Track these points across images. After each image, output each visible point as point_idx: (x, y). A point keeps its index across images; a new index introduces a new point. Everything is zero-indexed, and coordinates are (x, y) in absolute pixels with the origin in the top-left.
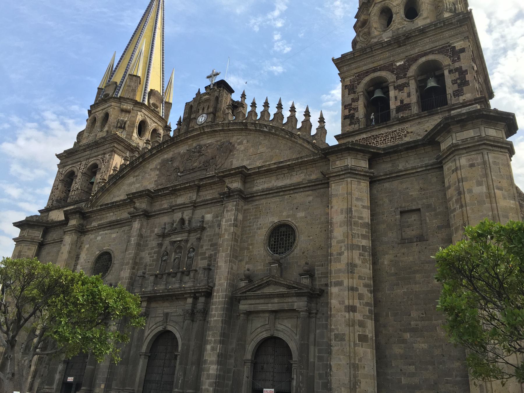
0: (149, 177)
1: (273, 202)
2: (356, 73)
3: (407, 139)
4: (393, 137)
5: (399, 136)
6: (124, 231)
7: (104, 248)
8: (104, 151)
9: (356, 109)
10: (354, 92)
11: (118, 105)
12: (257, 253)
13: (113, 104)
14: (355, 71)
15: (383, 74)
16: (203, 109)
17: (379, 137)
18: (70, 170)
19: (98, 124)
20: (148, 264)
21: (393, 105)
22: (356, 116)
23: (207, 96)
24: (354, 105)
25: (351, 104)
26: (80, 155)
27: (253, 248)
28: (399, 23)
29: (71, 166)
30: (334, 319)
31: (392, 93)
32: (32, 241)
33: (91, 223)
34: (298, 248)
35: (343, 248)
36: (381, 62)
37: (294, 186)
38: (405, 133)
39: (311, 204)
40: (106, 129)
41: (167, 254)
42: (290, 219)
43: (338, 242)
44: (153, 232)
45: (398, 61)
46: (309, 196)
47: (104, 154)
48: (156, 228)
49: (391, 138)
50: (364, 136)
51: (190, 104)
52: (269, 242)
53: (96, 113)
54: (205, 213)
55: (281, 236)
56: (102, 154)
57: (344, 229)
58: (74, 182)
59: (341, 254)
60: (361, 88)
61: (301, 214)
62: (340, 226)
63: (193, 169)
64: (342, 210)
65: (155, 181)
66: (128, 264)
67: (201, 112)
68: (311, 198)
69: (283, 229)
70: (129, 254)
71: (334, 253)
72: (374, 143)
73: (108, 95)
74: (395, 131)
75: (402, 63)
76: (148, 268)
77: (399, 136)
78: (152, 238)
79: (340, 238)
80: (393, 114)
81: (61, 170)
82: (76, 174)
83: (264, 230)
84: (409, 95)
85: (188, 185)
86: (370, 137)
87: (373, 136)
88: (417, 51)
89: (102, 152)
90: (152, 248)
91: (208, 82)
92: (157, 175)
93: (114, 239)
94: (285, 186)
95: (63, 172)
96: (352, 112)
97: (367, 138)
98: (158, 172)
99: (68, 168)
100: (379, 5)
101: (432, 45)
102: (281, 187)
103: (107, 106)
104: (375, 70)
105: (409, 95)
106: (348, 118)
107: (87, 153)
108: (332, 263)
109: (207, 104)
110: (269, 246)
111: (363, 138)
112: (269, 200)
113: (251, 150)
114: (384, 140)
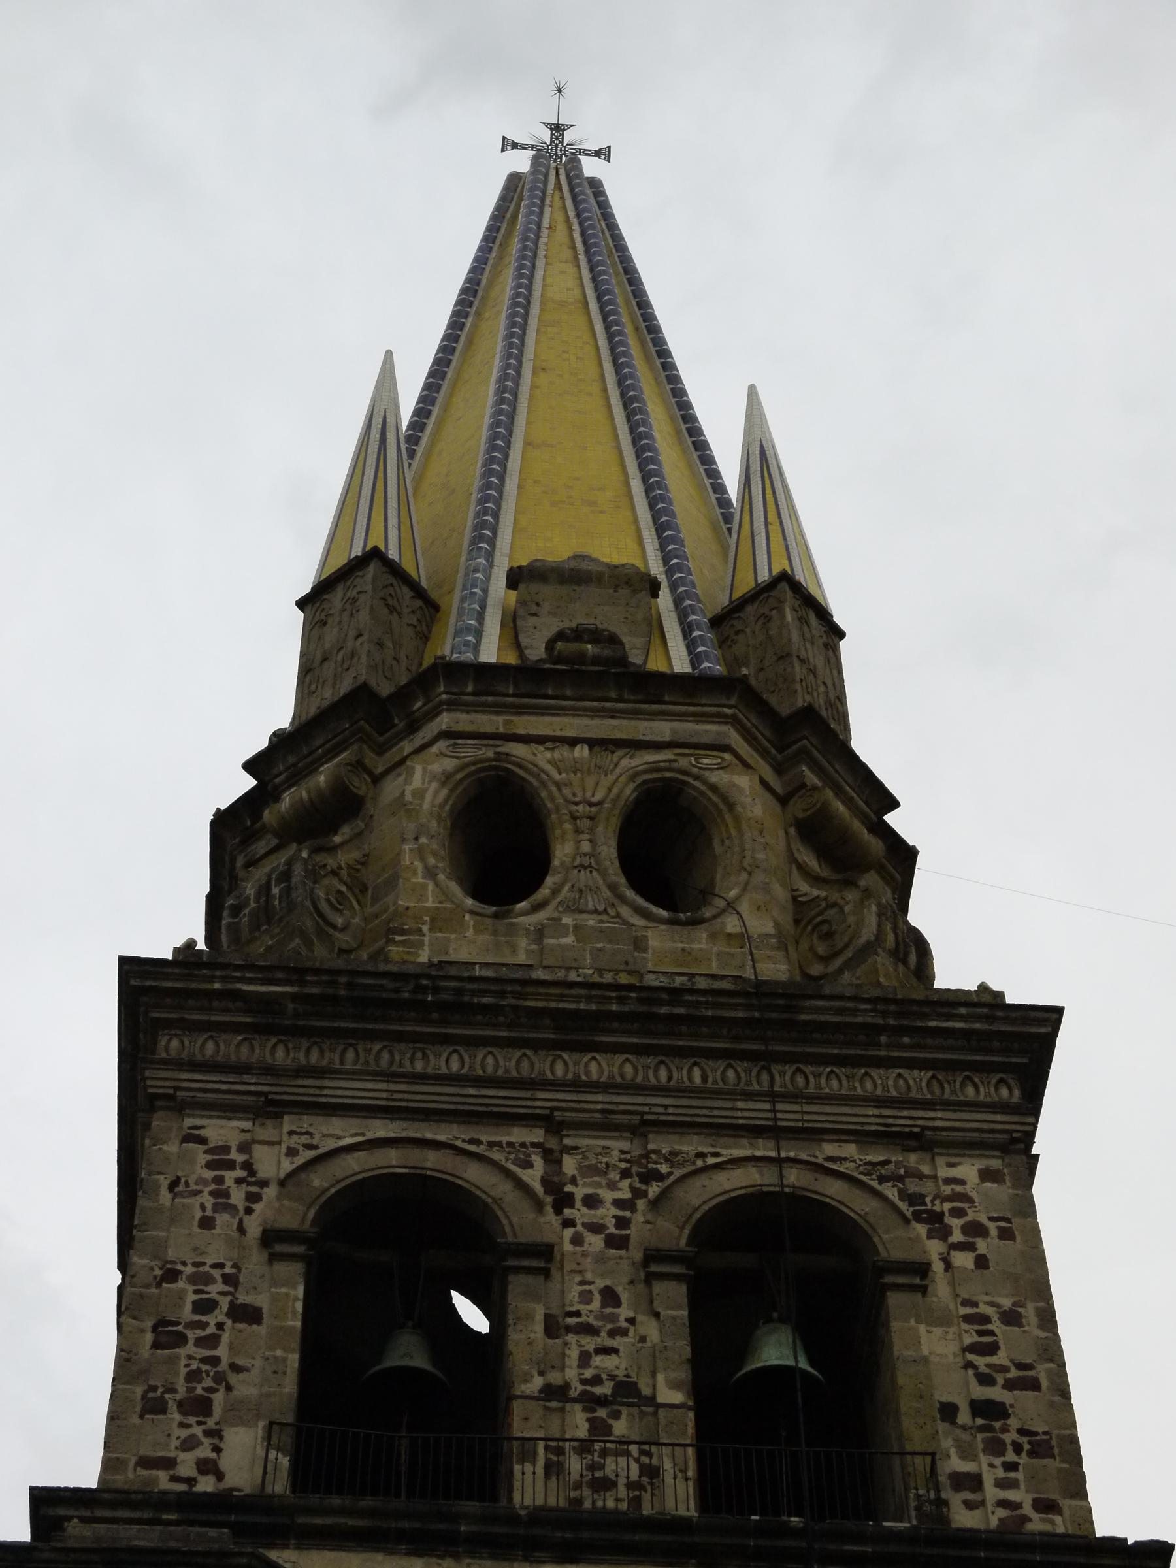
8: (903, 1119)
18: (392, 1160)
19: (583, 849)
53: (518, 750)
56: (863, 1137)
95: (271, 1163)
99: (347, 1146)
103: (663, 730)
107: (597, 1067)
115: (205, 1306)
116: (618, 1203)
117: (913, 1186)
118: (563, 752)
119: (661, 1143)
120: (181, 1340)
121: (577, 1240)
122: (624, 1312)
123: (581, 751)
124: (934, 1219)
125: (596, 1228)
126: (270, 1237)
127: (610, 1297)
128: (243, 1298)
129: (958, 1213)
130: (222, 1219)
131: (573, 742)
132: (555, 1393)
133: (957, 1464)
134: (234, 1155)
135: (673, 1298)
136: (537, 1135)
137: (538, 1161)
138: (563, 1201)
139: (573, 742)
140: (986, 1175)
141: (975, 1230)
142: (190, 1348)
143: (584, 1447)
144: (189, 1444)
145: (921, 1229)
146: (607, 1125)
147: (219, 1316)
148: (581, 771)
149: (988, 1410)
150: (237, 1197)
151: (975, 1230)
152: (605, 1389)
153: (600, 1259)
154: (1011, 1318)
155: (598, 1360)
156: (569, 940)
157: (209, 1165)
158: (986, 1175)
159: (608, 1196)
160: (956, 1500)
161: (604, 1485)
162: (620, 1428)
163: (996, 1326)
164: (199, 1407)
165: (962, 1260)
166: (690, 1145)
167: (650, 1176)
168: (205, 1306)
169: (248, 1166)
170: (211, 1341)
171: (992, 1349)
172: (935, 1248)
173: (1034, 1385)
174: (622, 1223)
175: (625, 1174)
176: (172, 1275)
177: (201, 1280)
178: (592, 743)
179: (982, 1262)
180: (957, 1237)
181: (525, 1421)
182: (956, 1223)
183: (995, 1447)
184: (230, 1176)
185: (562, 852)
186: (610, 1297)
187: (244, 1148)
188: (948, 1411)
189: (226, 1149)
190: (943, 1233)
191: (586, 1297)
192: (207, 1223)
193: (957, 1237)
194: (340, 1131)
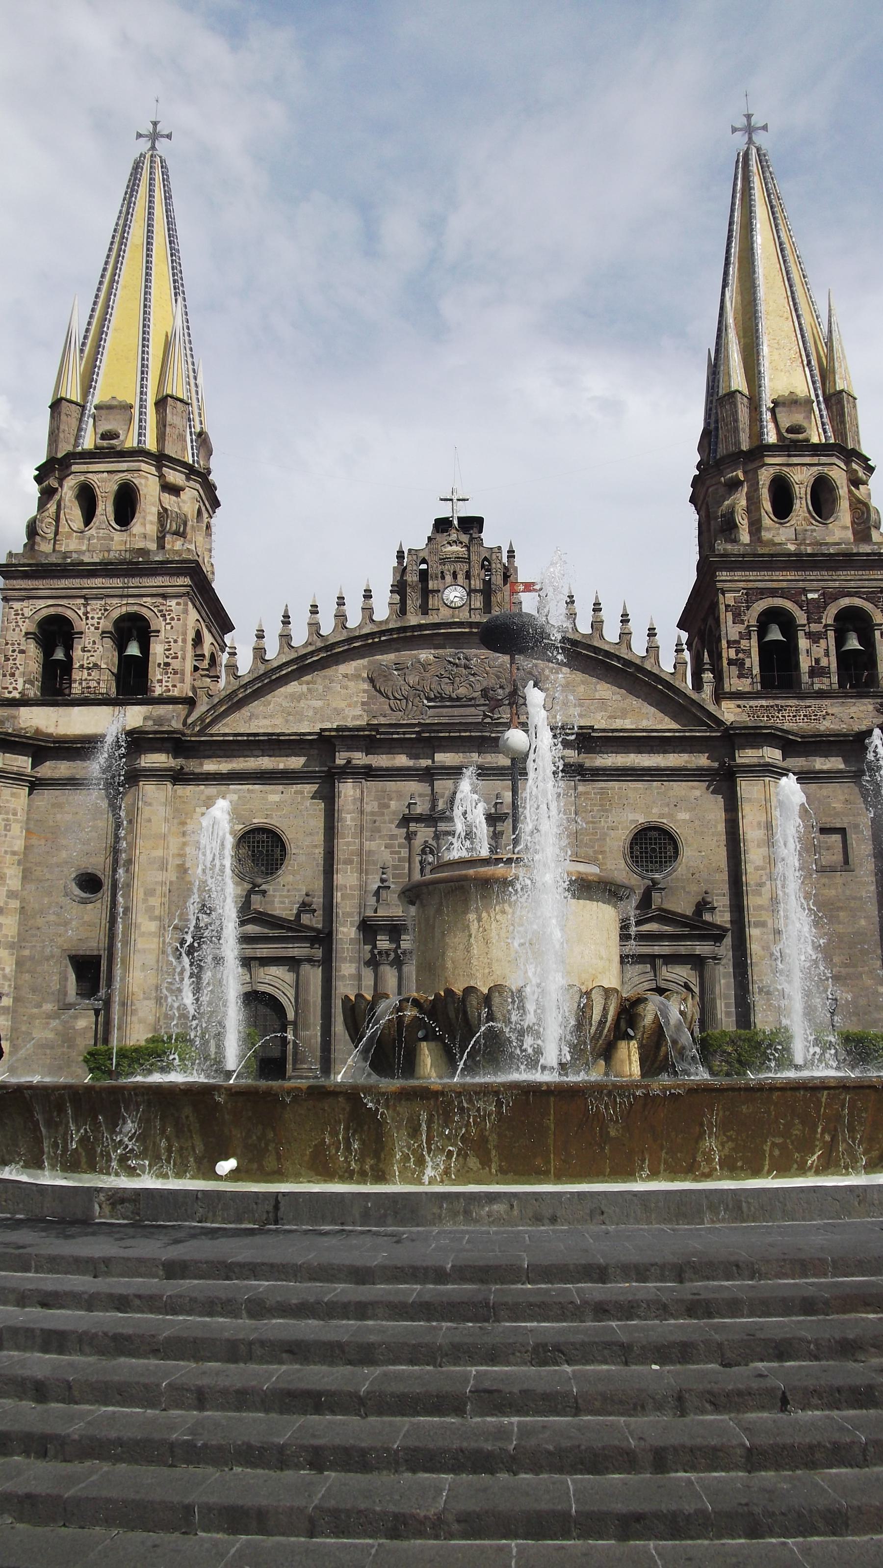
0: (343, 691)
1: (632, 789)
2: (744, 589)
3: (826, 725)
4: (804, 716)
5: (816, 715)
6: (302, 793)
7: (255, 821)
9: (748, 653)
10: (742, 622)
11: (153, 470)
12: (613, 867)
13: (144, 466)
14: (742, 585)
15: (788, 605)
16: (455, 575)
17: (785, 710)
18: (52, 611)
20: (390, 863)
21: (805, 664)
22: (748, 665)
23: (455, 548)
24: (744, 643)
25: (738, 642)
26: (77, 582)
27: (603, 858)
28: (805, 519)
29: (50, 602)
30: (755, 969)
31: (803, 643)
32: (17, 778)
33: (202, 765)
34: (683, 865)
35: (764, 878)
36: (784, 584)
37: (671, 770)
38: (824, 713)
39: (699, 802)
40: (136, 527)
41: (432, 852)
42: (665, 821)
43: (757, 869)
44: (388, 806)
45: (811, 591)
46: (693, 788)
47: (164, 596)
48: (391, 800)
49: (804, 716)
50: (764, 702)
51: (422, 555)
52: (632, 853)
53: (90, 476)
54: (503, 789)
55: (651, 844)
57: (764, 851)
58: (78, 647)
59: (761, 885)
60: (752, 616)
61: (683, 816)
62: (759, 846)
63: (458, 699)
64: (759, 823)
65: (363, 704)
66: (350, 862)
67: (449, 578)
68: (697, 793)
69: (655, 834)
70: (348, 844)
71: (752, 883)
72: (778, 717)
73: (115, 436)
74: (810, 707)
75: (816, 596)
76: (389, 871)
77: (816, 715)
78: (387, 818)
79: (759, 862)
80: (805, 678)
81: (17, 605)
82: (79, 625)
83: (620, 831)
84: (827, 654)
85: (468, 734)
86: (772, 706)
87: (777, 706)
88: (837, 584)
89: (154, 591)
90: (393, 837)
91: (445, 511)
92: (365, 691)
93: (278, 805)
94: (657, 769)
95: (28, 613)
96: (741, 655)
97: (767, 706)
98: (366, 686)
99: (41, 608)
100: (772, 470)
101: (860, 584)
102: (649, 769)
103: (124, 466)
104: (773, 593)
105: (827, 654)
106: (735, 665)
107: (98, 582)
108: (750, 897)
109: (466, 567)
110: (632, 857)
111: (762, 706)
112: (624, 785)
113: (582, 688)
114: (794, 716)
115: (14, 651)
116: (99, 618)
117: (161, 608)
118: (100, 475)
119: (109, 601)
120: (9, 659)
121: (89, 628)
122: (96, 646)
123: (105, 474)
124: (164, 616)
125: (92, 625)
126: (27, 634)
127: (94, 642)
128: (22, 647)
129: (169, 615)
130: (17, 629)
131: (103, 472)
132: (82, 666)
133: (160, 677)
134: (20, 612)
135: (109, 643)
136: (82, 601)
137: (82, 608)
138: (87, 618)
139: (103, 472)
140: (178, 604)
141: (172, 619)
142: (11, 661)
143: (86, 680)
144: (11, 683)
145: (161, 619)
146: (97, 598)
147: (16, 653)
148: (105, 481)
149: (167, 664)
150: (20, 623)
151: (172, 619)
152: (91, 666)
153: (93, 633)
154: (176, 641)
155: (90, 658)
156: (95, 541)
157: (15, 615)
158: (178, 604)
159: (96, 616)
160: (157, 685)
161: (89, 687)
162: (93, 674)
163: (172, 644)
164: (13, 675)
165: (168, 627)
166: (115, 601)
167: (106, 610)
168: (14, 651)
169: (23, 614)
170: (15, 660)
171: (170, 649)
172: (164, 623)
173: (177, 658)
174: (99, 623)
175: (100, 610)
176: (7, 644)
177: (13, 644)
178: (108, 472)
179: (172, 628)
180: (168, 621)
181: (76, 675)
182: (168, 617)
183: (167, 673)
184: (19, 617)
185: (99, 510)
186: (94, 642)
187: (22, 610)
188: (159, 665)
189: (17, 610)
190: (165, 620)
191: (89, 643)
192: (14, 630)
193: (168, 621)
194: (42, 603)
